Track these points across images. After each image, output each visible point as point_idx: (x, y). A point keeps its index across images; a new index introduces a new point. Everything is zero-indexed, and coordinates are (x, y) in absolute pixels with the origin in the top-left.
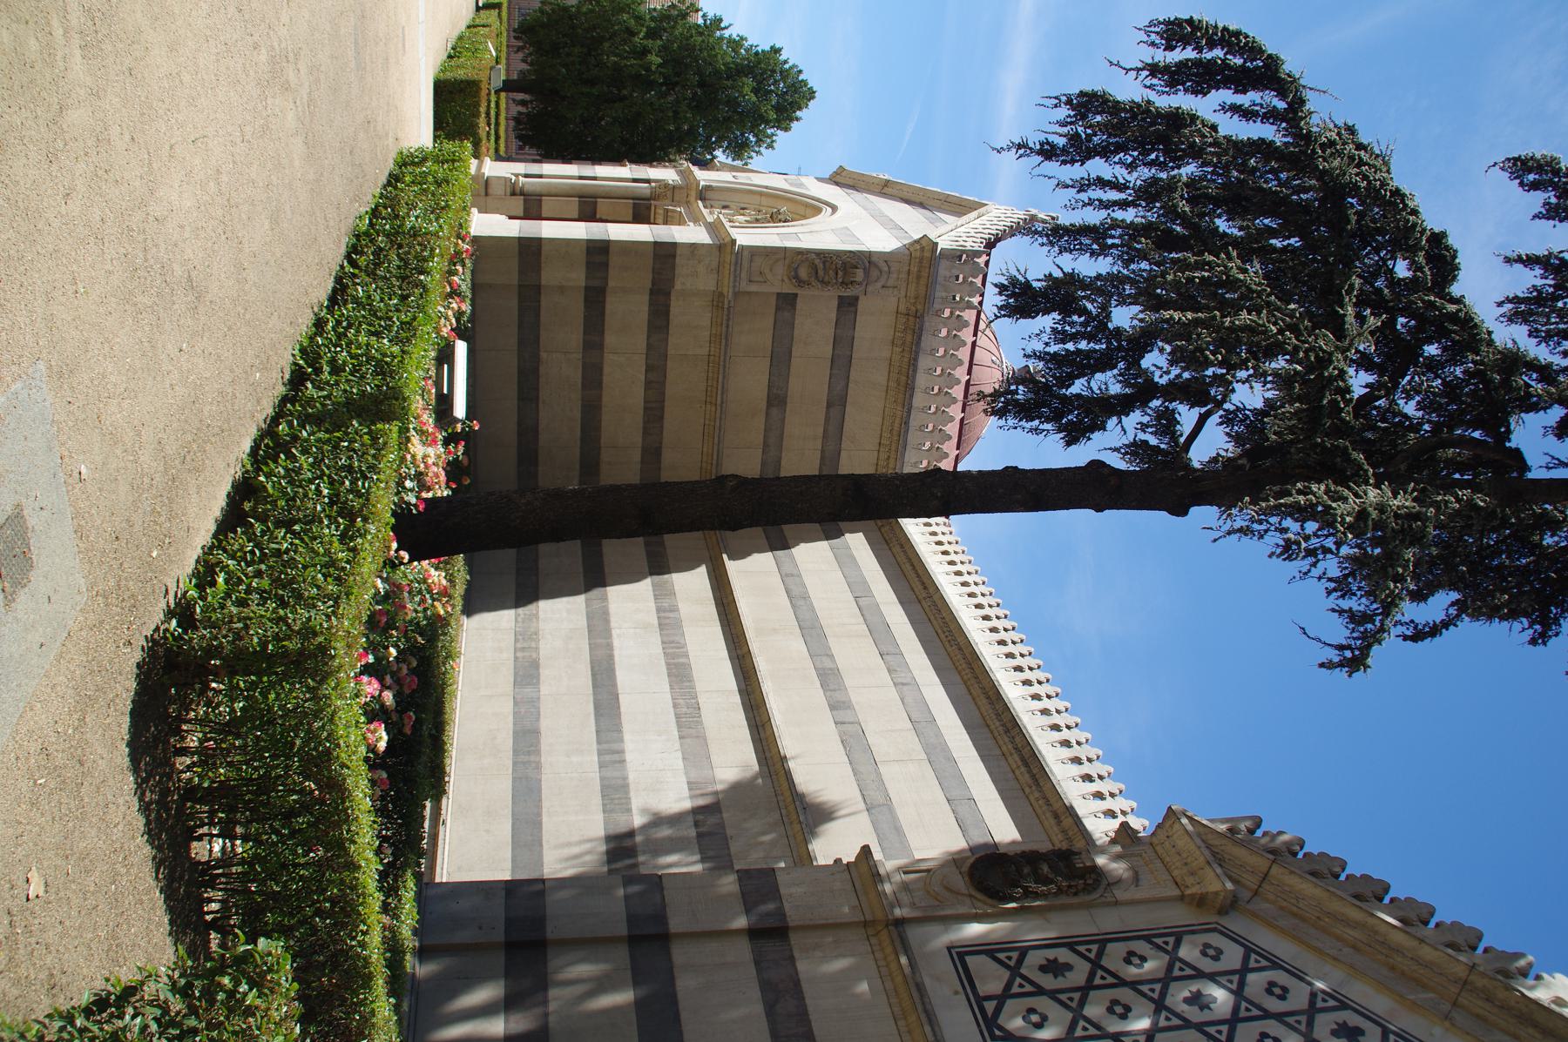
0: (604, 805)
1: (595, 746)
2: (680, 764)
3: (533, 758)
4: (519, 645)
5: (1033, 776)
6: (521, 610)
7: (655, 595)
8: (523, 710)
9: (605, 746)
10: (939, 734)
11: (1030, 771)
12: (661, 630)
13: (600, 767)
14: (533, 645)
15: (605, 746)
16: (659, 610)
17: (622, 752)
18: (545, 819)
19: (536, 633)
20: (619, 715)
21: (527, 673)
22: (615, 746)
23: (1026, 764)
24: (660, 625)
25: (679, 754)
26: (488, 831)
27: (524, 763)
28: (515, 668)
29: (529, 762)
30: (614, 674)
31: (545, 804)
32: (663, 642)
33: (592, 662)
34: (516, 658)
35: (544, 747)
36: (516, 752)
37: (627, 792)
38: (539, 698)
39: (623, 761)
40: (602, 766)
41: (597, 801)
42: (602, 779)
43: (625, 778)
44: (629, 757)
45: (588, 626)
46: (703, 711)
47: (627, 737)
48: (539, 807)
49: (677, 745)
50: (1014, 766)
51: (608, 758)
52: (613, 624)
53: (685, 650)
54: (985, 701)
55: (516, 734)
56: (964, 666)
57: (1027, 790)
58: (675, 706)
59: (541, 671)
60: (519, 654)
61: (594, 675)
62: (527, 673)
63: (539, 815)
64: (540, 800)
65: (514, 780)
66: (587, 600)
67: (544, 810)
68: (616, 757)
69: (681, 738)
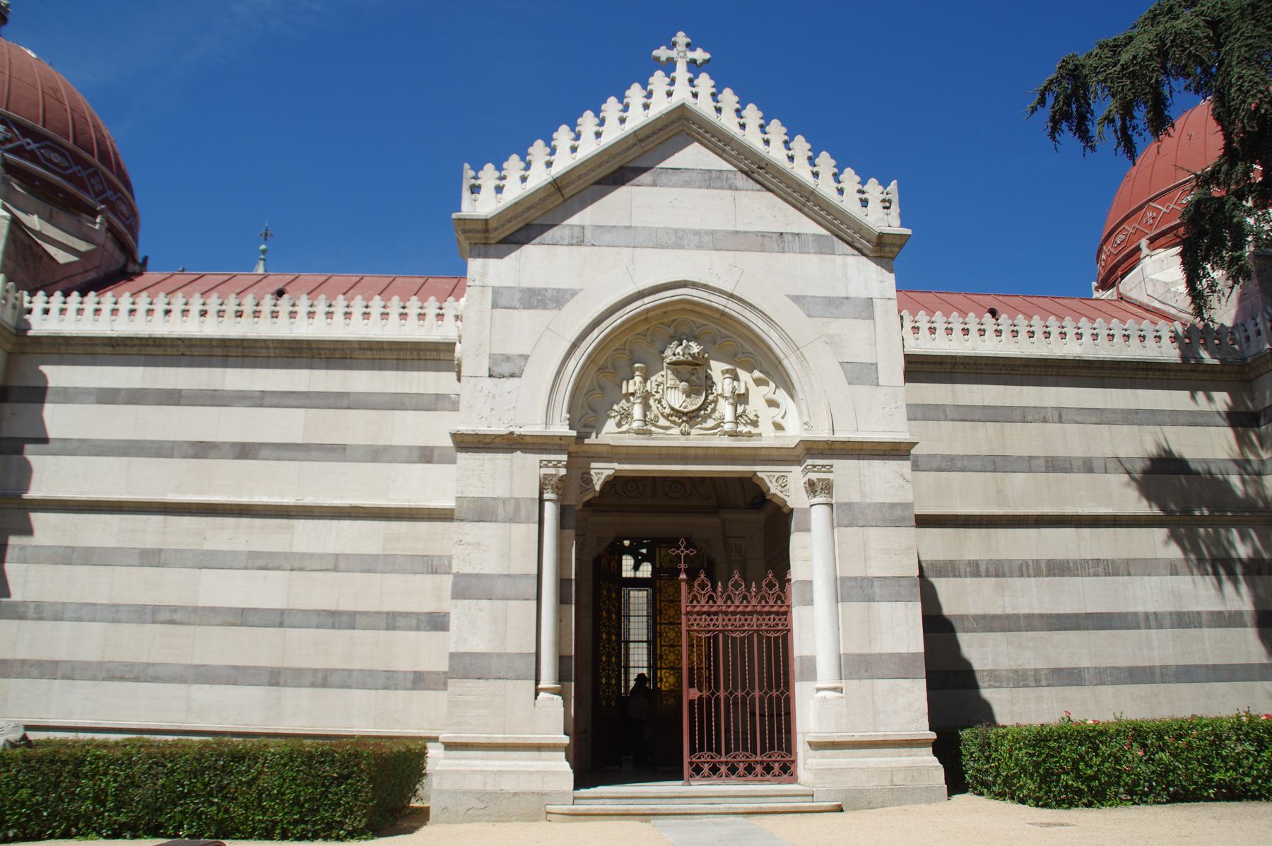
0: (1195, 627)
1: (1143, 631)
2: (1154, 578)
3: (1158, 671)
4: (1033, 684)
5: (1159, 370)
6: (980, 684)
7: (954, 576)
8: (1109, 678)
9: (1142, 624)
10: (1114, 411)
11: (1155, 370)
12: (1004, 576)
13: (1162, 628)
14: (1032, 673)
15: (1142, 624)
16: (987, 576)
17: (1146, 614)
18: (1210, 662)
19: (1016, 671)
20: (1110, 614)
21: (1021, 679)
22: (1142, 618)
23: (1148, 370)
24: (997, 576)
25: (1146, 578)
26: (1224, 696)
27: (1162, 676)
28: (1062, 686)
29: (1161, 673)
30: (1064, 614)
31: (1198, 662)
32: (1022, 576)
33: (1051, 630)
34: (1048, 685)
35: (1146, 663)
36: (1154, 682)
37: (1183, 613)
38: (1096, 668)
39: (1155, 614)
40: (1161, 627)
41: (1192, 632)
42: (1172, 627)
43: (1171, 613)
44: (1151, 609)
45: (1003, 631)
46: (1102, 557)
47: (1131, 609)
48: (1201, 666)
49: (1138, 578)
50: (1144, 376)
51: (1153, 623)
52: (999, 612)
53: (1030, 563)
54: (1084, 371)
55: (1133, 683)
56: (1044, 370)
57: (1166, 377)
58: (1096, 575)
59: (1063, 667)
60: (1044, 682)
61: (1066, 629)
62: (1021, 679)
63: (1207, 666)
64: (1195, 666)
65: (1178, 682)
66: (966, 631)
67: (1203, 663)
68: (1152, 618)
69: (1129, 574)
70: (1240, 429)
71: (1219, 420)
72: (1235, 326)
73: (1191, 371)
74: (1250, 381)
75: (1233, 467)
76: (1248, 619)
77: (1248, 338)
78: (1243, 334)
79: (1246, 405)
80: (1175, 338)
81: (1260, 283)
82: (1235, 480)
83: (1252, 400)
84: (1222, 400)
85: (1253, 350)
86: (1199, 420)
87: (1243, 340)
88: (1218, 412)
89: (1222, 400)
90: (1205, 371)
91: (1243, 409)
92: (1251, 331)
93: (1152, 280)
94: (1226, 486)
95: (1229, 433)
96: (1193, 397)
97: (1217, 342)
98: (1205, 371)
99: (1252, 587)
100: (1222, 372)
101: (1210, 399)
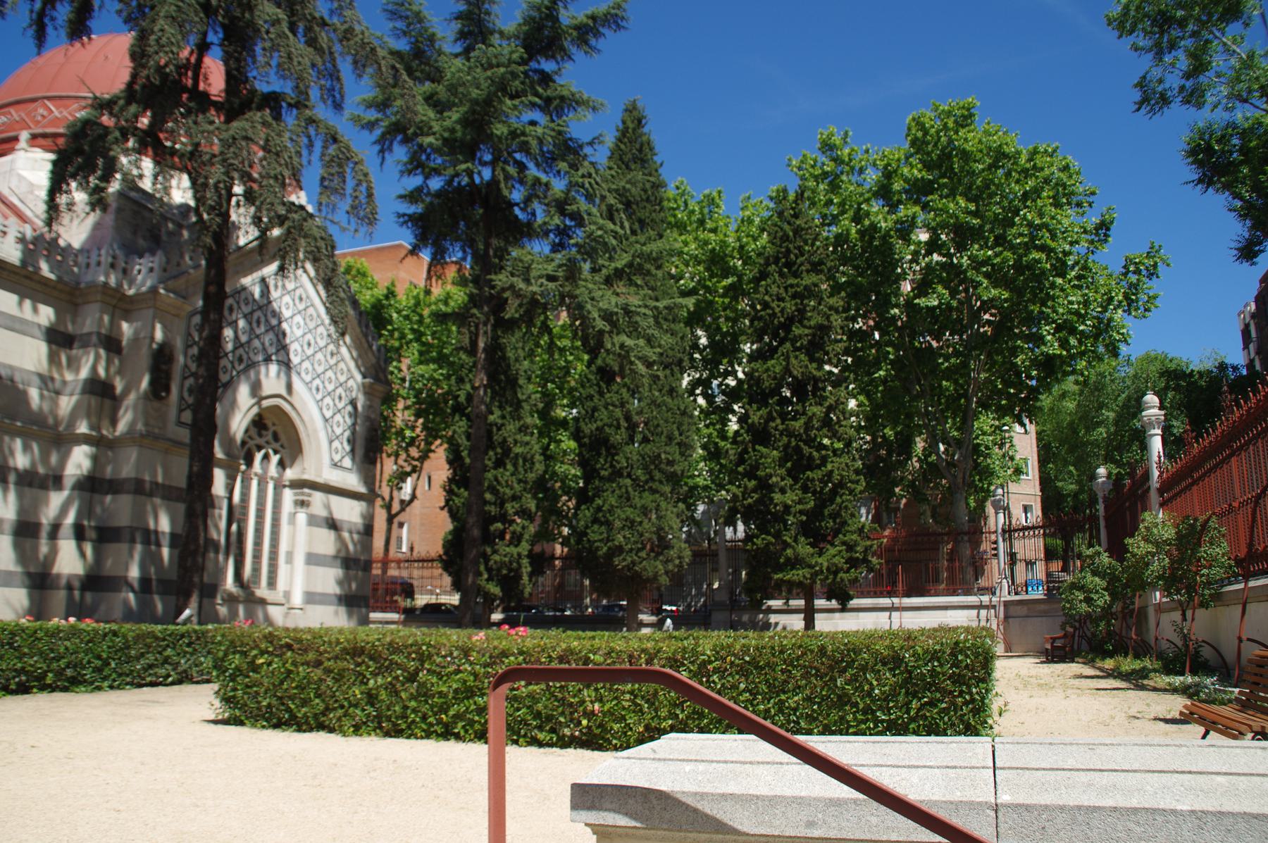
70: (54, 347)
71: (37, 332)
72: (81, 251)
73: (26, 277)
74: (76, 305)
75: (36, 380)
76: (8, 527)
77: (88, 265)
78: (86, 261)
79: (66, 326)
80: (22, 240)
81: (117, 219)
82: (34, 394)
83: (74, 323)
84: (46, 315)
85: (89, 278)
86: (17, 326)
87: (84, 265)
88: (39, 326)
89: (46, 315)
90: (39, 282)
91: (62, 329)
92: (94, 260)
93: (19, 176)
94: (23, 396)
95: (42, 348)
96: (20, 304)
97: (59, 258)
98: (39, 282)
99: (20, 497)
100: (54, 288)
101: (35, 310)
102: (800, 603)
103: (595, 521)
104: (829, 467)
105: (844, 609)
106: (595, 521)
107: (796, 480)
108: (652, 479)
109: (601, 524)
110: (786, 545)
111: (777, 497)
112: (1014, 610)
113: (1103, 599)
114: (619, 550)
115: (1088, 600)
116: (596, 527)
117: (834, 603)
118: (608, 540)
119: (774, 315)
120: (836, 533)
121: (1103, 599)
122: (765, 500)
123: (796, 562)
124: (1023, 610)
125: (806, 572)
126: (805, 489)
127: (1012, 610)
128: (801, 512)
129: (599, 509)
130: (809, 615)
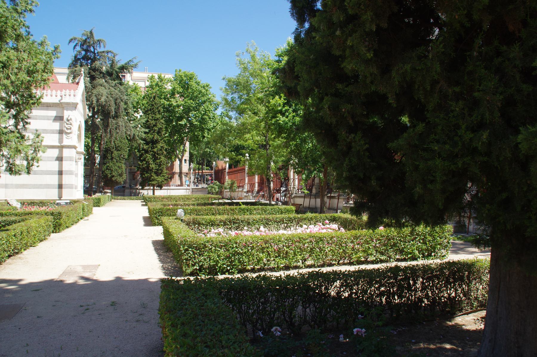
102: (152, 188)
103: (107, 169)
104: (161, 160)
105: (161, 189)
106: (107, 169)
107: (154, 162)
108: (120, 160)
109: (109, 170)
110: (152, 176)
111: (150, 165)
112: (194, 190)
113: (217, 190)
114: (113, 176)
115: (215, 190)
116: (107, 170)
117: (158, 188)
118: (111, 174)
119: (150, 124)
120: (161, 173)
121: (217, 190)
122: (148, 167)
123: (153, 180)
124: (196, 190)
125: (157, 182)
126: (156, 164)
127: (194, 190)
128: (156, 169)
129: (108, 166)
130: (154, 190)
